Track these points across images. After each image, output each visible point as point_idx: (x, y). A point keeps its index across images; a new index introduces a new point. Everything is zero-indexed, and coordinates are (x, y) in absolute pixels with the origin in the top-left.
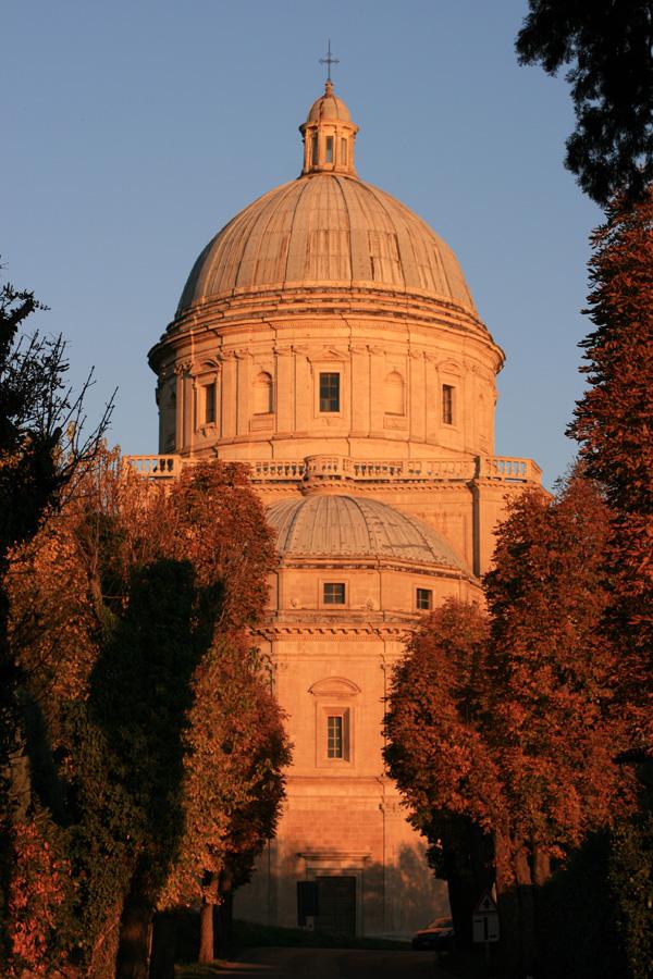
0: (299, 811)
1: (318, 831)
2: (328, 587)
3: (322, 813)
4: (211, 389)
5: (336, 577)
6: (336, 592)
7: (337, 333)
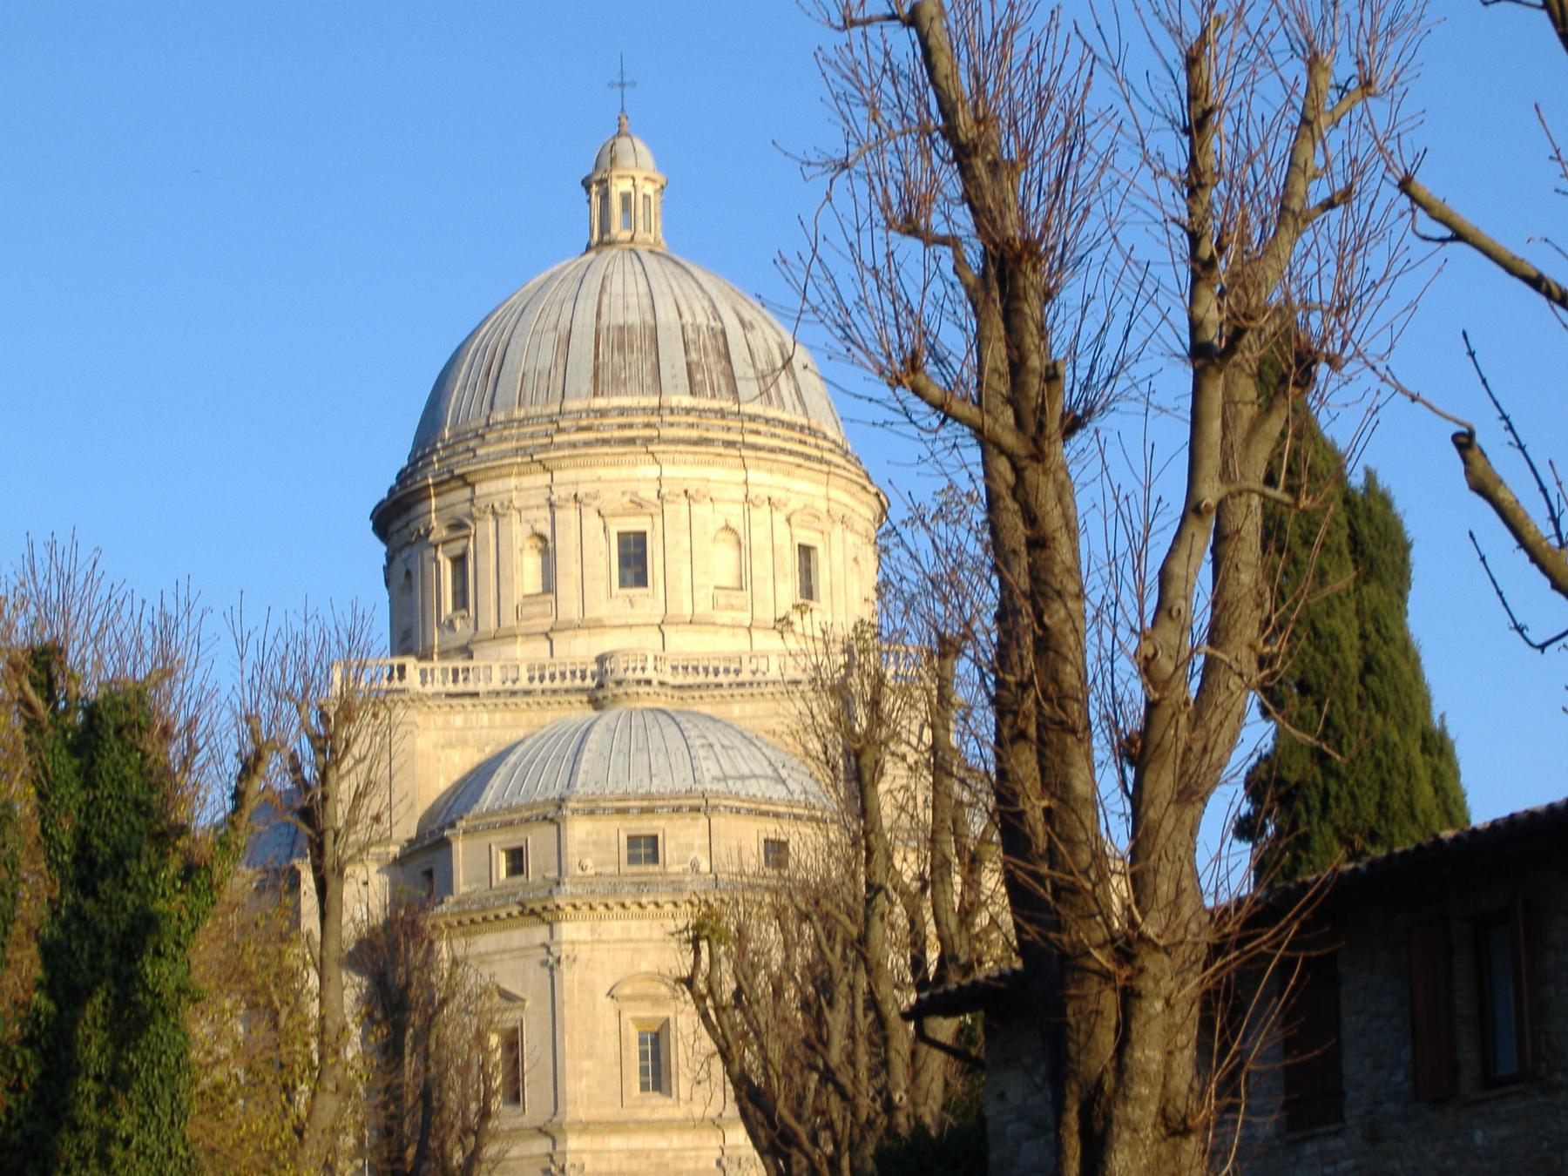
2: (633, 841)
4: (459, 562)
5: (645, 826)
6: (646, 848)
7: (640, 473)
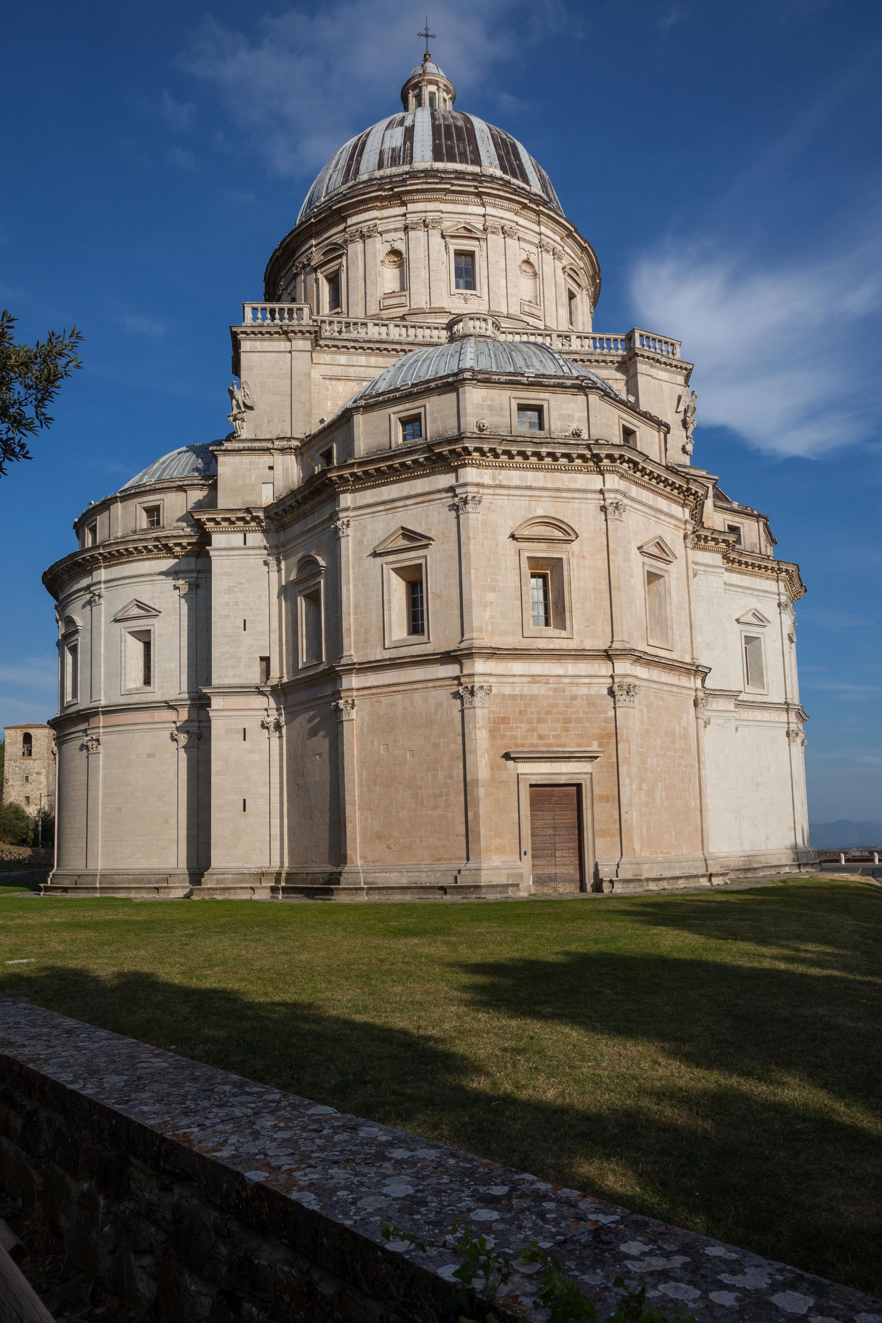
0: (504, 696)
3: (534, 697)
4: (334, 280)
5: (532, 396)
7: (471, 212)
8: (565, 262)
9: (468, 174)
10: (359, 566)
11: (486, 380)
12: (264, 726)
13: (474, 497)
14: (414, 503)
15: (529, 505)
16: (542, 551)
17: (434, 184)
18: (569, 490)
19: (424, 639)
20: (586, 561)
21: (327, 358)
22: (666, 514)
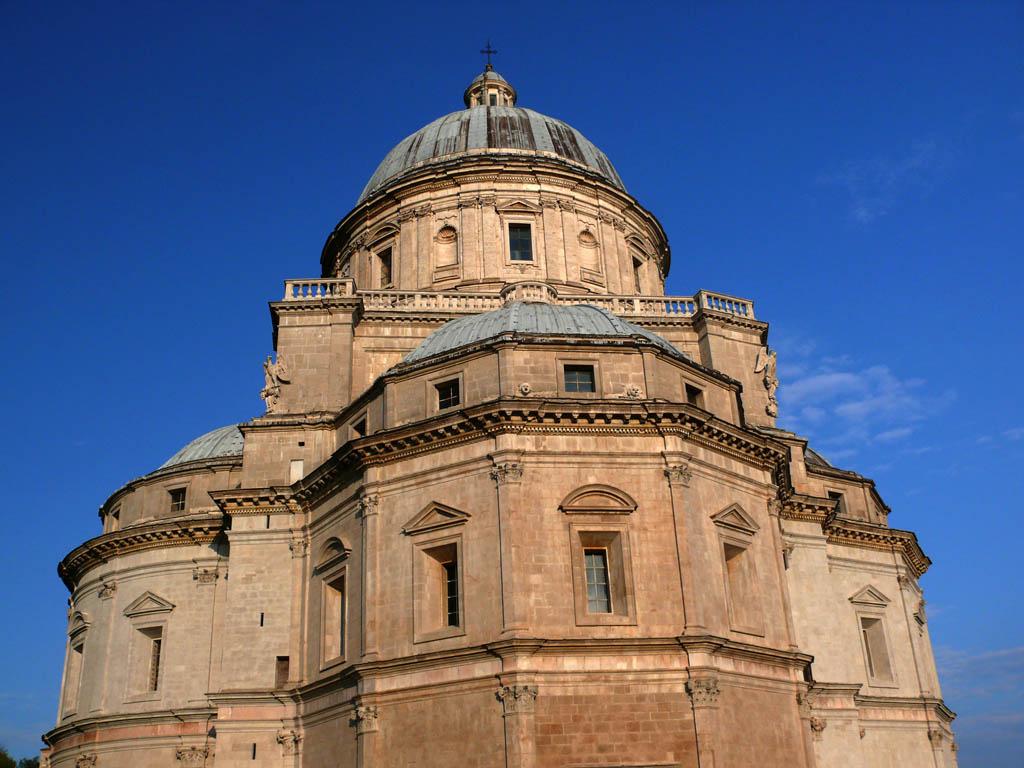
0: (554, 698)
1: (587, 730)
2: (568, 369)
3: (591, 699)
5: (580, 357)
8: (627, 232)
9: (522, 156)
10: (387, 548)
11: (528, 341)
12: (281, 741)
13: (514, 466)
14: (447, 475)
15: (579, 473)
16: (595, 525)
17: (488, 165)
18: (624, 455)
19: (459, 631)
20: (649, 534)
21: (371, 331)
22: (743, 479)
